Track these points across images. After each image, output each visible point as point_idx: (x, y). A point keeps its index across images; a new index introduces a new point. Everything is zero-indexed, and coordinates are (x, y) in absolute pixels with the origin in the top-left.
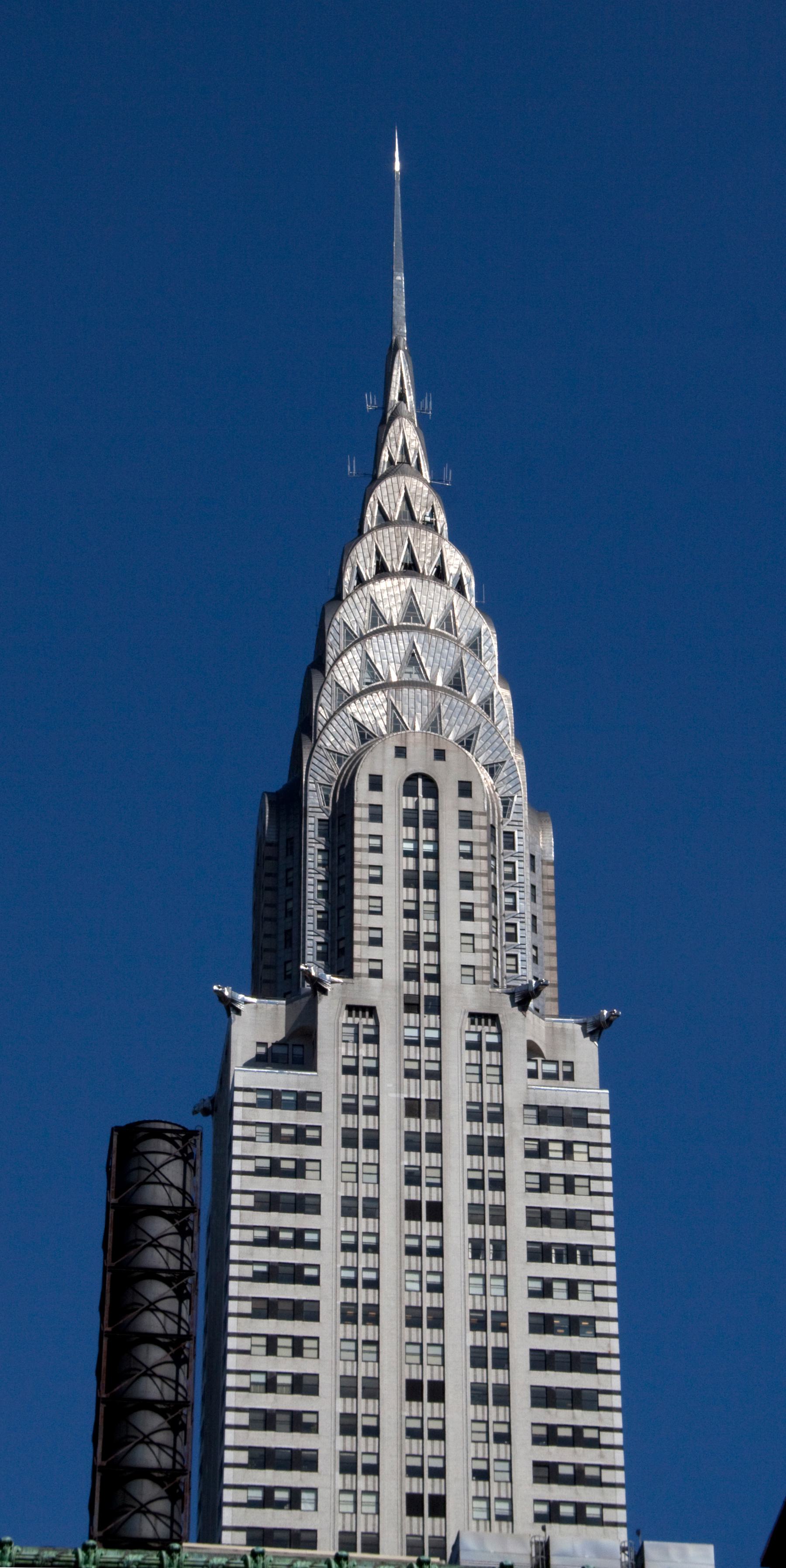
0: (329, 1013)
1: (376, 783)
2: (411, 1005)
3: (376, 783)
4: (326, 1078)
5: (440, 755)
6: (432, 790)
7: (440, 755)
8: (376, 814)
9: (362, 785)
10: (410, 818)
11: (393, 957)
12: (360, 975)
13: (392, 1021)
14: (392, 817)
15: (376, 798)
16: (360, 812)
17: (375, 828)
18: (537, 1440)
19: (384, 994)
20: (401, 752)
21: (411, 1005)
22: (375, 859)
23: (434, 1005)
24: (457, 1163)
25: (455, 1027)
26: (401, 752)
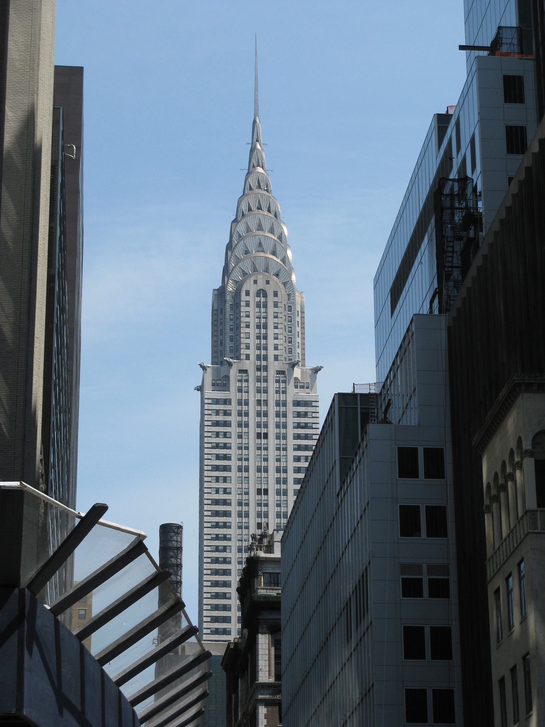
0: (233, 373)
1: (247, 293)
2: (258, 369)
3: (247, 293)
4: (233, 394)
5: (268, 282)
6: (265, 295)
7: (268, 282)
8: (248, 305)
9: (243, 294)
10: (258, 305)
11: (253, 352)
12: (243, 359)
13: (252, 374)
14: (252, 304)
15: (247, 298)
16: (243, 304)
17: (247, 309)
18: (295, 449)
19: (249, 365)
20: (255, 282)
21: (258, 369)
22: (247, 320)
23: (266, 368)
24: (272, 420)
25: (272, 375)
26: (255, 282)
